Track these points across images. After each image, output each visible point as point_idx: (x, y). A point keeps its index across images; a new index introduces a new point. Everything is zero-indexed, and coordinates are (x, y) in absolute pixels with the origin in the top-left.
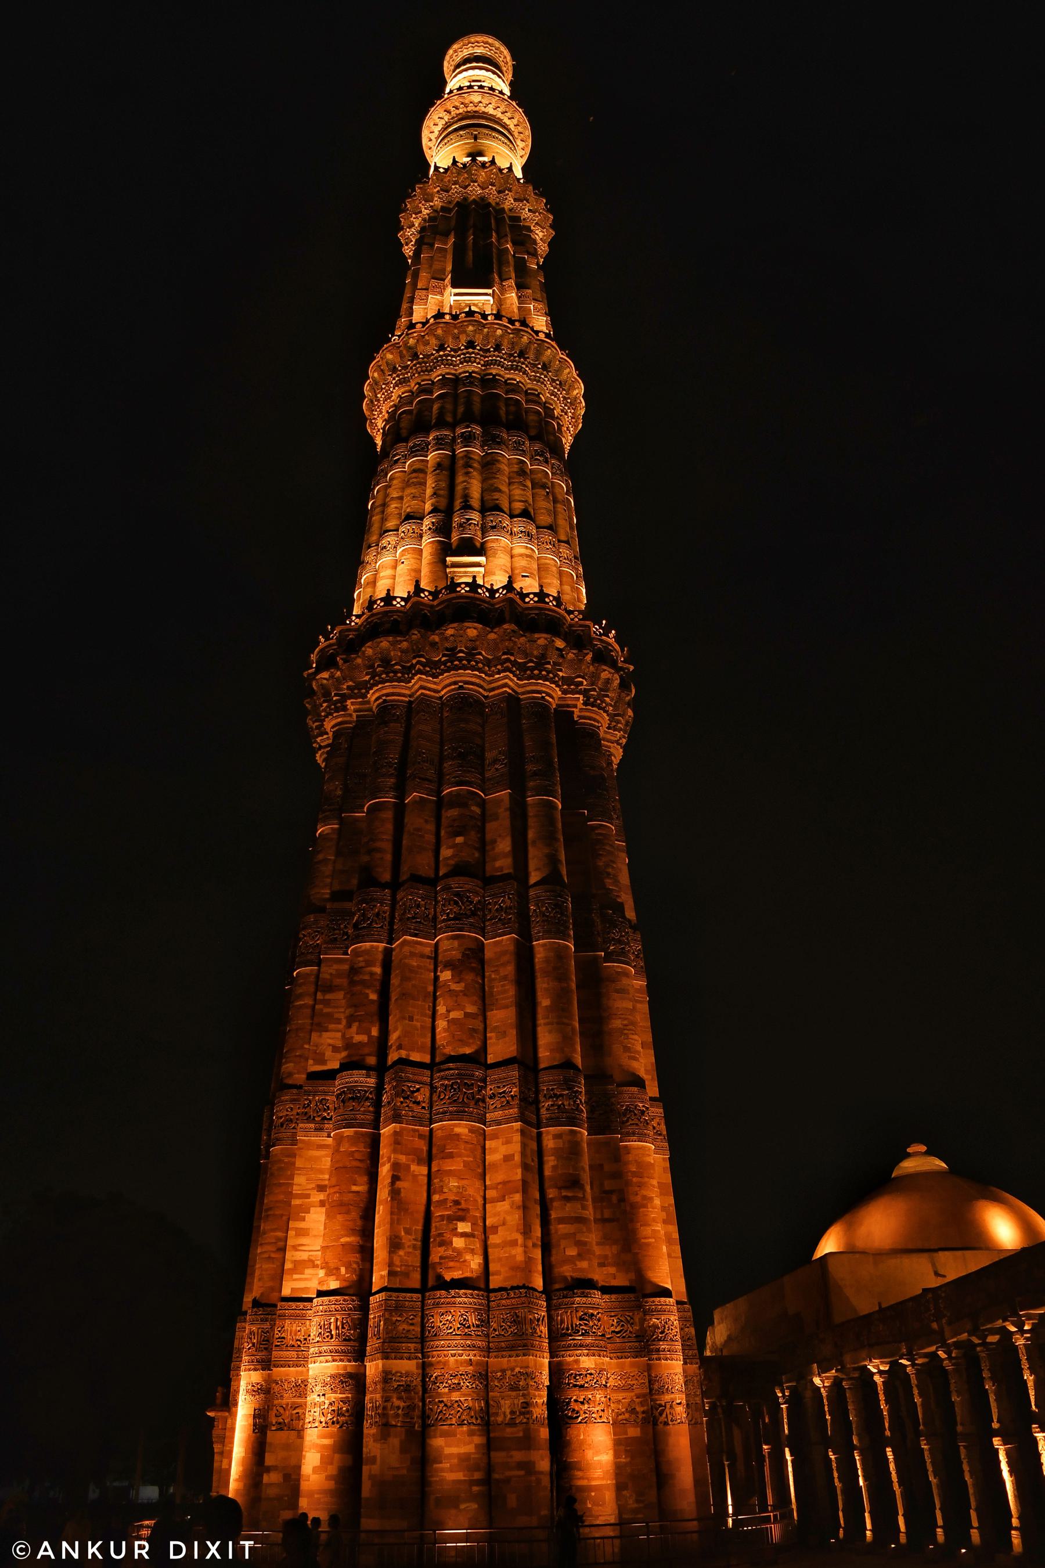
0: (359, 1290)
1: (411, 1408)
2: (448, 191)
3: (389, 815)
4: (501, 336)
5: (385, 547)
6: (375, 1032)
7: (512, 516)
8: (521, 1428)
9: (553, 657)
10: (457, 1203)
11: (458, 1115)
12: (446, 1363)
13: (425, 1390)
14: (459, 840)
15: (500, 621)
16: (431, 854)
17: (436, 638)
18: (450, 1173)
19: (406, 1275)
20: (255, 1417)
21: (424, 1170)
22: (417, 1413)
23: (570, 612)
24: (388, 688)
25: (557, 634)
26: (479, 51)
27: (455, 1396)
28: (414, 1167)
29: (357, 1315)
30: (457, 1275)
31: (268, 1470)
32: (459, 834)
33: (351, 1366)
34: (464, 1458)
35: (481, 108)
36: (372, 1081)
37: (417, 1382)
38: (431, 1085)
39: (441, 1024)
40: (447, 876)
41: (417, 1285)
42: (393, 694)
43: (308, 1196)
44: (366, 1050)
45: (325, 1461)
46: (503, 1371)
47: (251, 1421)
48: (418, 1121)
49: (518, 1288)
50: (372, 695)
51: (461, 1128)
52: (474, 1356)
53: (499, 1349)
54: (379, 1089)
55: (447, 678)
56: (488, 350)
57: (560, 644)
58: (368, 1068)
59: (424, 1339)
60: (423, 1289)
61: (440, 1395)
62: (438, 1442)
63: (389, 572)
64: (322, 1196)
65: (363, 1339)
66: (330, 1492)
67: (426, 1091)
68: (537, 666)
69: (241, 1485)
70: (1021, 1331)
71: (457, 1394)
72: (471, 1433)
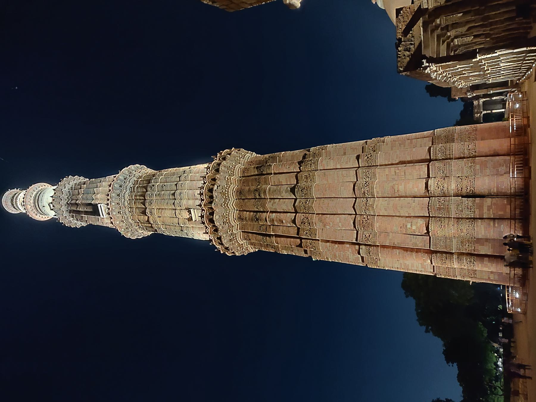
0: (431, 252)
1: (468, 241)
3: (279, 239)
6: (348, 246)
8: (475, 210)
11: (372, 225)
14: (284, 221)
15: (212, 208)
16: (290, 228)
23: (205, 183)
24: (239, 239)
27: (465, 231)
28: (390, 237)
32: (282, 222)
35: (32, 205)
36: (363, 247)
39: (343, 228)
40: (296, 225)
44: (354, 249)
45: (486, 266)
51: (377, 225)
54: (366, 245)
57: (215, 188)
62: (480, 236)
71: (465, 229)
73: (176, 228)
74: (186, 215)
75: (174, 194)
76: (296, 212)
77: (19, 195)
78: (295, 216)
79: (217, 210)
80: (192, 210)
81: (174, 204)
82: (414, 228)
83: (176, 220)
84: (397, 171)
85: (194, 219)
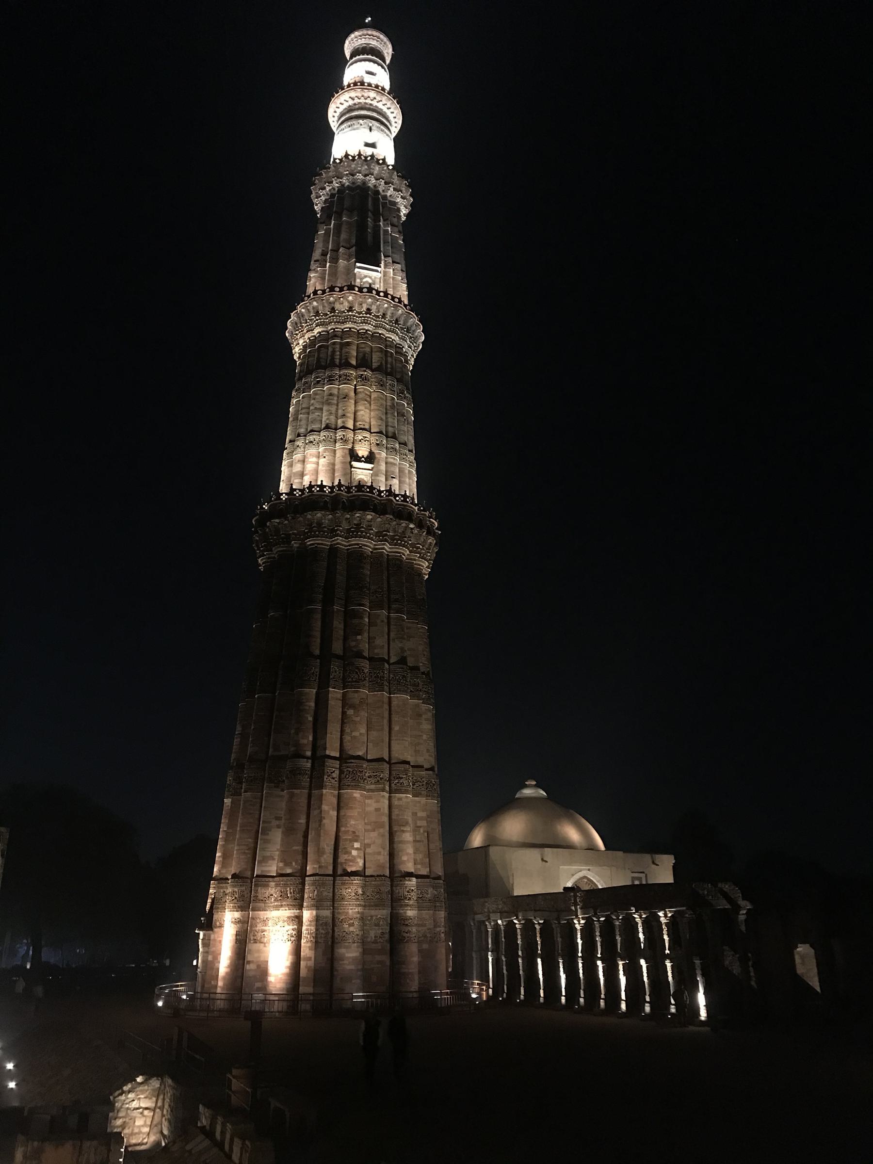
1: (327, 933)
2: (353, 175)
4: (387, 308)
5: (311, 442)
7: (387, 437)
9: (408, 534)
10: (354, 832)
11: (356, 787)
12: (348, 913)
13: (334, 925)
16: (341, 641)
17: (348, 516)
18: (351, 817)
19: (327, 867)
20: (236, 935)
21: (335, 813)
22: (330, 935)
25: (411, 521)
26: (374, 43)
27: (352, 929)
28: (331, 812)
29: (300, 887)
30: (354, 869)
31: (249, 962)
33: (296, 912)
34: (354, 959)
35: (374, 103)
37: (330, 921)
38: (340, 769)
41: (331, 873)
42: (322, 544)
43: (270, 822)
46: (372, 917)
47: (234, 937)
48: (333, 788)
49: (380, 876)
50: (309, 542)
51: (357, 794)
52: (360, 909)
53: (370, 906)
55: (354, 541)
56: (378, 317)
57: (412, 526)
58: (308, 758)
59: (334, 900)
60: (334, 875)
61: (343, 928)
63: (314, 459)
64: (277, 822)
65: (302, 899)
66: (287, 974)
67: (337, 772)
68: (398, 539)
69: (228, 970)
70: (618, 919)
72: (358, 947)
73: (333, 418)
74: (362, 451)
75: (394, 437)
76: (370, 659)
77: (379, 64)
78: (365, 658)
79: (379, 519)
80: (370, 466)
81: (380, 432)
82: (354, 853)
83: (350, 424)
84: (422, 831)
85: (355, 464)
